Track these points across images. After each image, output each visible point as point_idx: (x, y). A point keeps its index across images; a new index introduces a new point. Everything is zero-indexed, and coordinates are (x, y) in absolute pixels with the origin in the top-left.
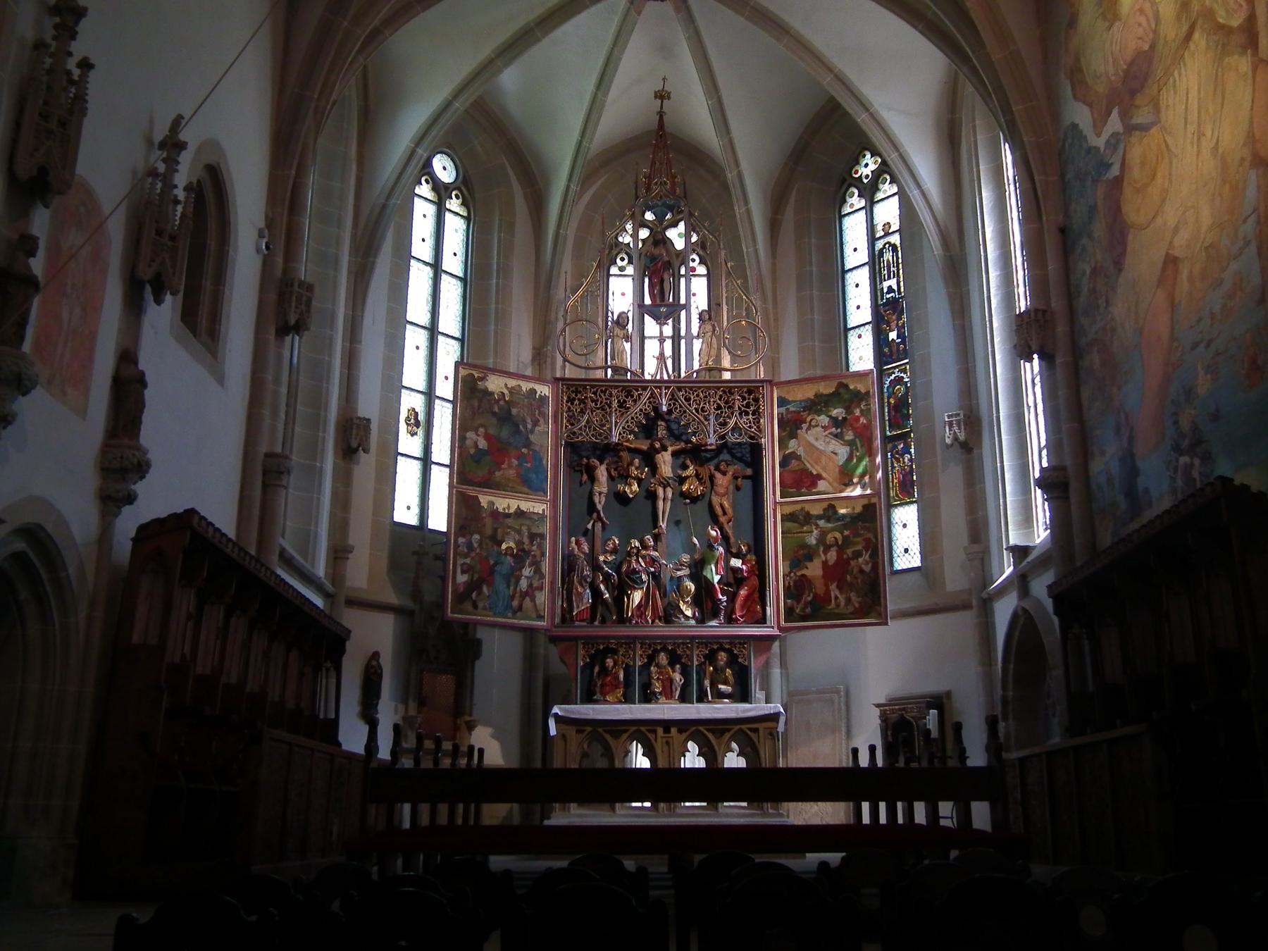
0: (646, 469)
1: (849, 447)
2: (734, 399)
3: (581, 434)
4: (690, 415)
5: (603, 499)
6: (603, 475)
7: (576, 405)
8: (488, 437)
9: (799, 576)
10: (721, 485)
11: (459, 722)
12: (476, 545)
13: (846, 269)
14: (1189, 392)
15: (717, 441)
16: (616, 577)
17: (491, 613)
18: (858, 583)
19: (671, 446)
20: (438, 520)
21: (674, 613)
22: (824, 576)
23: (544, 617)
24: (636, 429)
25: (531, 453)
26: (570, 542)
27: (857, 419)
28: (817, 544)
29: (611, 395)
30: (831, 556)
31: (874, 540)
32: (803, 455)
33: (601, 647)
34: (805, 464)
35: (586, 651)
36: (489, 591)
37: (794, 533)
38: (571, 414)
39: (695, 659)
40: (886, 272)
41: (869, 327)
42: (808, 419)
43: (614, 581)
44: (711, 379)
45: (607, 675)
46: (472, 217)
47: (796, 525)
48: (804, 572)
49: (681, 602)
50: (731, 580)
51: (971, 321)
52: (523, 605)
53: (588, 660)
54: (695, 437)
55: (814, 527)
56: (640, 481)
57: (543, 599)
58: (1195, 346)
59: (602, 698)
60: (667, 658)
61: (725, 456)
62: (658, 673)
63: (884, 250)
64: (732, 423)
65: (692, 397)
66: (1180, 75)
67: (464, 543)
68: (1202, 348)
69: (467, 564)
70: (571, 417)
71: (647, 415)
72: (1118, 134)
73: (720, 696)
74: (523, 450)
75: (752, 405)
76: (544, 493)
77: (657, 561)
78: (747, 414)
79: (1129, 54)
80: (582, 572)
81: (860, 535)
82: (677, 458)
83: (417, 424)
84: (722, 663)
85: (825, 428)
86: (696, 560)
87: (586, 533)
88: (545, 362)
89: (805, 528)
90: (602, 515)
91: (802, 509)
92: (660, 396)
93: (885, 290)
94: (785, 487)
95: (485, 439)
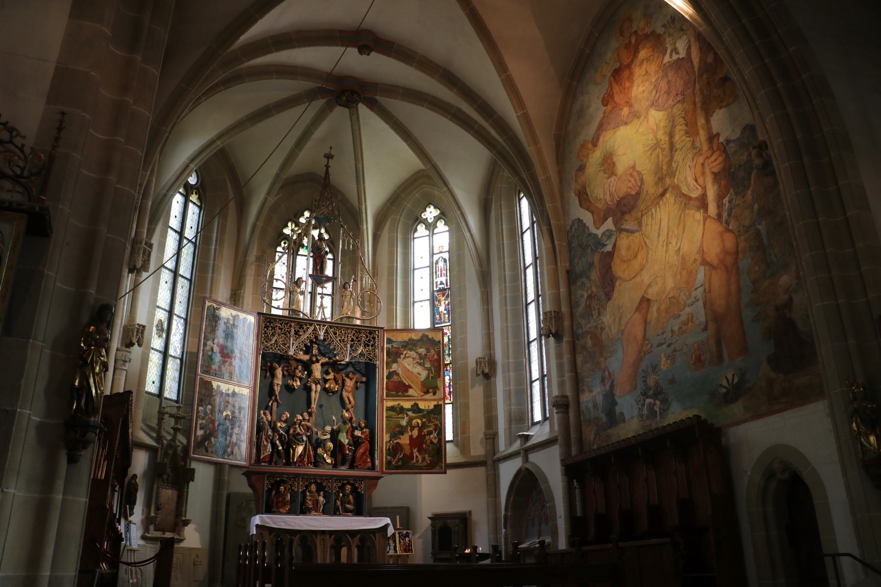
0: (306, 372)
2: (362, 337)
3: (272, 348)
4: (336, 343)
5: (279, 388)
6: (280, 374)
12: (209, 412)
14: (655, 368)
16: (287, 437)
17: (215, 456)
20: (171, 391)
22: (410, 444)
24: (304, 349)
29: (291, 326)
31: (440, 425)
33: (278, 479)
35: (269, 481)
38: (266, 335)
41: (428, 303)
42: (405, 352)
44: (349, 323)
46: (203, 206)
47: (394, 413)
48: (398, 441)
53: (270, 487)
55: (405, 415)
56: (301, 379)
58: (660, 345)
61: (350, 369)
63: (439, 261)
66: (656, 211)
67: (203, 410)
68: (664, 346)
69: (203, 423)
70: (266, 337)
72: (611, 230)
78: (369, 346)
79: (621, 194)
81: (432, 422)
83: (162, 330)
88: (239, 299)
89: (400, 416)
90: (278, 398)
93: (439, 283)
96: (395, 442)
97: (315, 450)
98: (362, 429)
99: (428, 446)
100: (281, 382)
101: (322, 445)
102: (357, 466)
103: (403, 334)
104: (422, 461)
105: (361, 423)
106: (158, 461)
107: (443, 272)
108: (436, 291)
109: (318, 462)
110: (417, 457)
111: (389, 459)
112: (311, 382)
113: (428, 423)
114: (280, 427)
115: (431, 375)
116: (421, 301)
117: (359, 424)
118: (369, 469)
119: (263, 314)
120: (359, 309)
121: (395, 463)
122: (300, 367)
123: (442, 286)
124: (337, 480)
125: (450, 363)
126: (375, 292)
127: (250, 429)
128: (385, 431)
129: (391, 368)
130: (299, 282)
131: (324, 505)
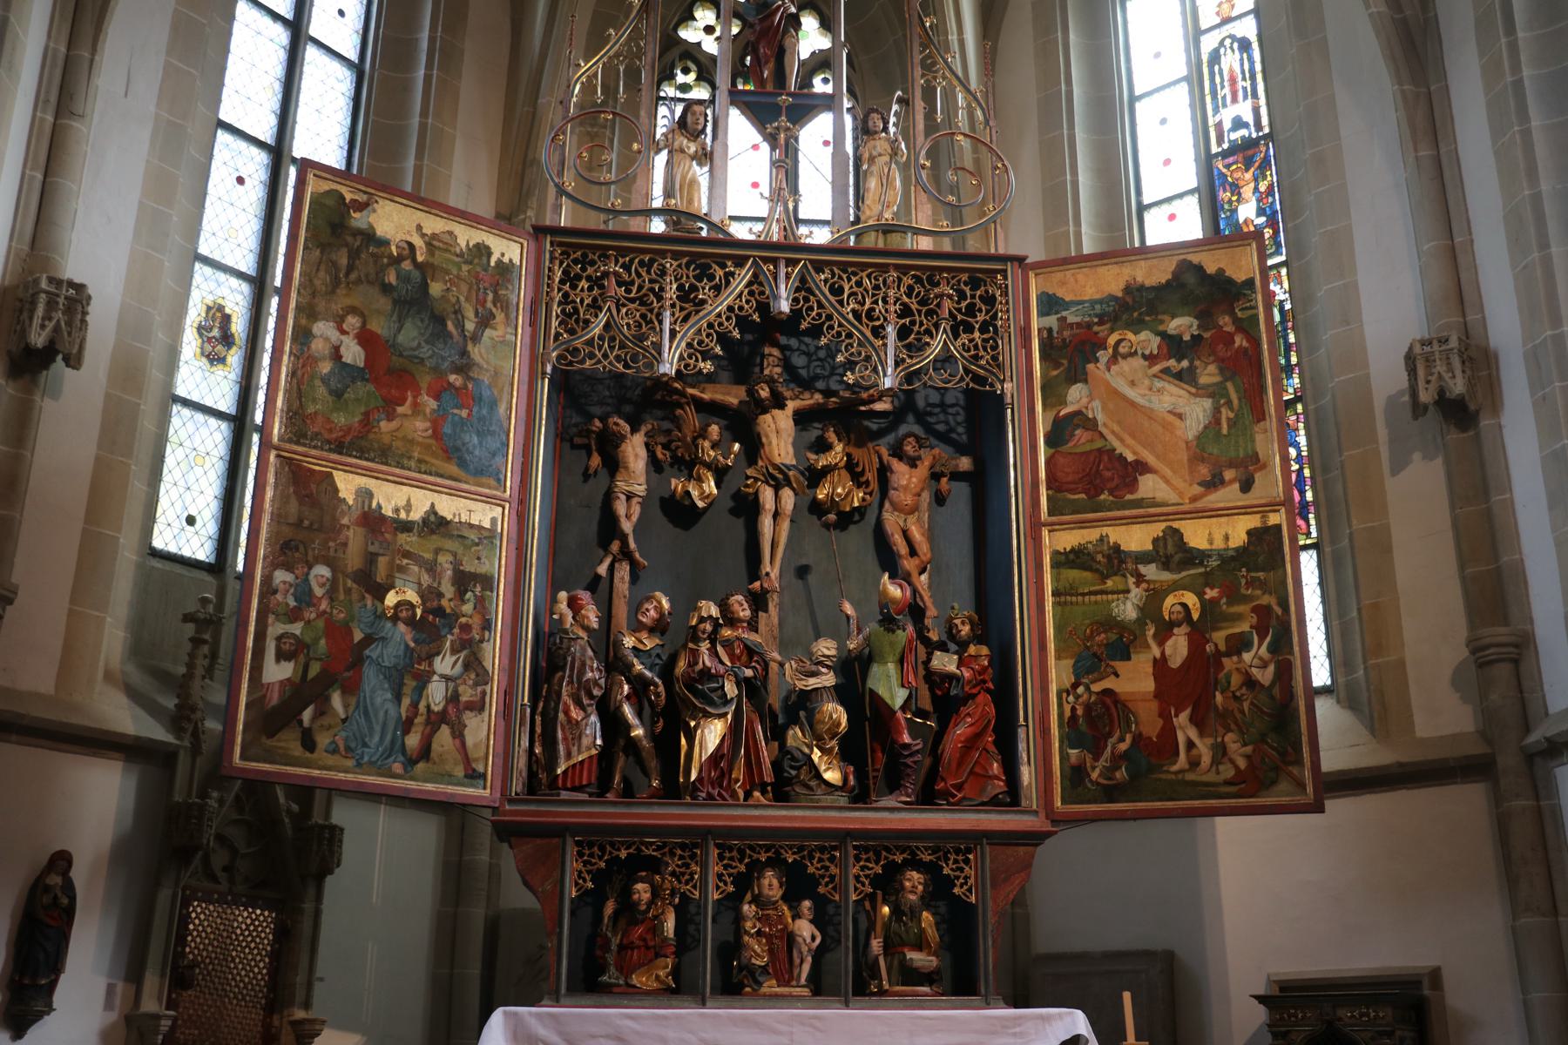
0: (737, 446)
1: (1210, 400)
2: (941, 296)
3: (592, 356)
4: (840, 325)
5: (636, 510)
7: (582, 290)
8: (366, 339)
9: (1097, 693)
10: (906, 488)
11: (276, 1023)
12: (319, 592)
13: (1137, 92)
15: (900, 384)
16: (661, 689)
17: (350, 763)
18: (1242, 712)
19: (791, 399)
21: (797, 776)
22: (1158, 695)
23: (484, 776)
24: (718, 350)
25: (470, 386)
26: (554, 600)
27: (1230, 339)
28: (1138, 619)
30: (1175, 648)
31: (1278, 610)
32: (1100, 418)
33: (623, 854)
34: (1106, 440)
35: (585, 863)
36: (346, 706)
37: (1083, 595)
38: (569, 308)
39: (852, 889)
40: (1227, 91)
41: (1192, 203)
42: (1112, 340)
43: (658, 695)
45: (636, 923)
47: (1087, 575)
48: (1108, 683)
49: (815, 749)
51: (1456, 149)
52: (435, 746)
53: (590, 885)
54: (853, 373)
55: (1131, 580)
56: (720, 474)
57: (485, 733)
59: (621, 982)
60: (781, 887)
61: (910, 426)
62: (759, 919)
63: (1222, 50)
64: (936, 346)
65: (846, 288)
67: (291, 585)
70: (570, 316)
71: (743, 323)
73: (911, 976)
74: (452, 378)
75: (980, 310)
76: (498, 480)
77: (759, 654)
78: (969, 329)
80: (582, 672)
81: (1246, 599)
82: (804, 429)
83: (227, 339)
84: (912, 897)
85: (1151, 359)
86: (849, 650)
87: (594, 585)
89: (1110, 583)
90: (632, 545)
91: (1102, 539)
92: (775, 279)
93: (1227, 125)
94: (1059, 490)
95: (360, 343)
96: (1096, 688)
97: (777, 733)
98: (963, 646)
99: (1235, 698)
100: (644, 487)
101: (802, 714)
102: (946, 795)
103: (1102, 270)
104: (1216, 762)
105: (957, 622)
106: (178, 798)
107: (1241, 84)
108: (1217, 155)
109: (789, 781)
110: (1190, 745)
111: (1073, 760)
112: (756, 480)
113: (1229, 604)
114: (634, 648)
115: (1225, 413)
116: (1169, 200)
118: (995, 803)
119: (555, 231)
120: (923, 197)
121: (1100, 775)
122: (714, 429)
123: (1244, 132)
124: (866, 849)
125: (1297, 399)
126: (985, 138)
127: (506, 661)
128: (1051, 646)
129: (1064, 403)
130: (689, 119)
131: (819, 955)
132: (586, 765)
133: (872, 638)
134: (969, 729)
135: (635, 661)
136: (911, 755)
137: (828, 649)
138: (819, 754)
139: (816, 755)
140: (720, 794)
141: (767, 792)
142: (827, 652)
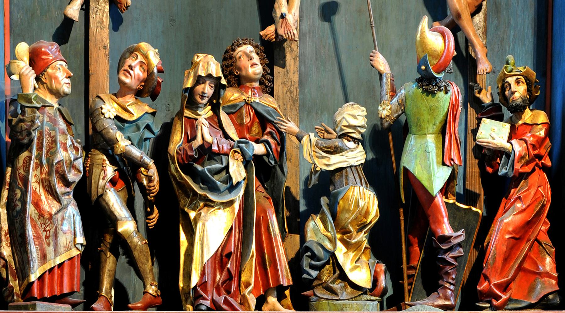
49: (339, 244)
50: (477, 187)
80: (52, 153)
101: (324, 201)
105: (511, 80)
109: (309, 284)
117: (503, 89)
132: (66, 270)
133: (408, 103)
134: (519, 216)
135: (119, 135)
136: (451, 249)
137: (355, 117)
138: (345, 250)
139: (340, 251)
140: (226, 302)
141: (285, 297)
142: (353, 122)
